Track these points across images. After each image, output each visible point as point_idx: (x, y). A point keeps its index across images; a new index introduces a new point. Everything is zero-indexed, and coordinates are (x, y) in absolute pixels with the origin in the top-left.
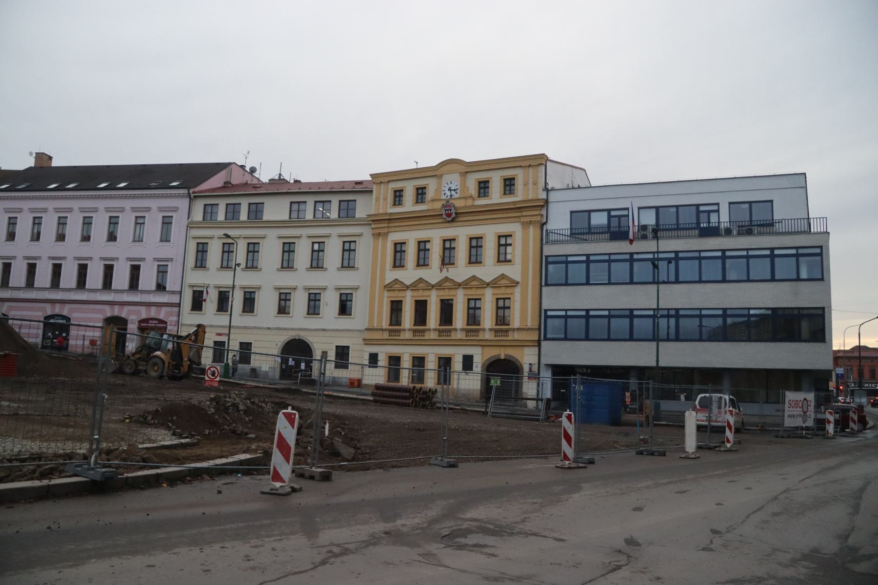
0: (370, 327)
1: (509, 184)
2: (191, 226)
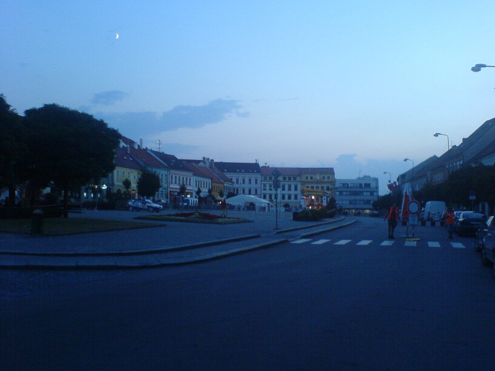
2: (261, 181)
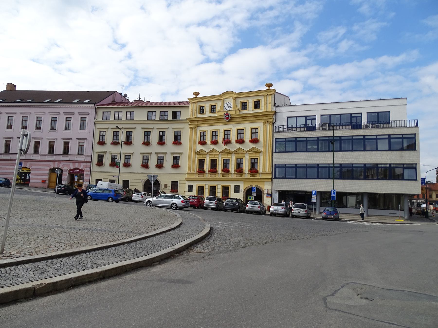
0: (188, 172)
1: (257, 105)
